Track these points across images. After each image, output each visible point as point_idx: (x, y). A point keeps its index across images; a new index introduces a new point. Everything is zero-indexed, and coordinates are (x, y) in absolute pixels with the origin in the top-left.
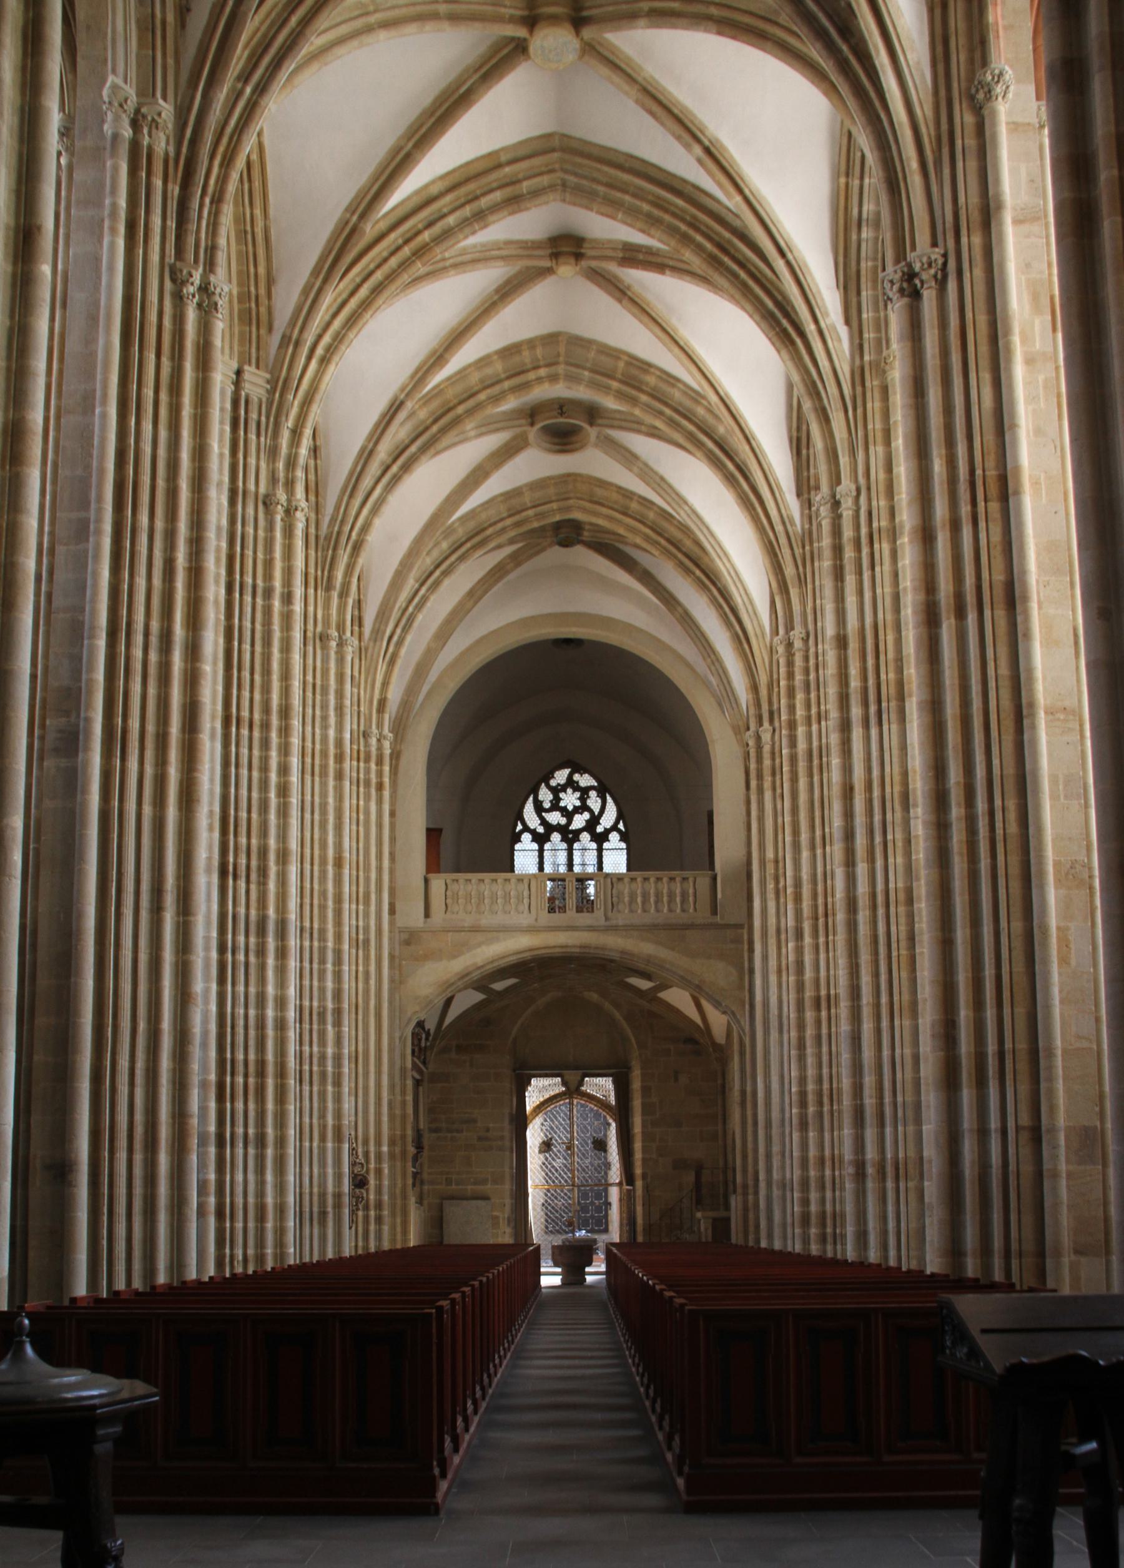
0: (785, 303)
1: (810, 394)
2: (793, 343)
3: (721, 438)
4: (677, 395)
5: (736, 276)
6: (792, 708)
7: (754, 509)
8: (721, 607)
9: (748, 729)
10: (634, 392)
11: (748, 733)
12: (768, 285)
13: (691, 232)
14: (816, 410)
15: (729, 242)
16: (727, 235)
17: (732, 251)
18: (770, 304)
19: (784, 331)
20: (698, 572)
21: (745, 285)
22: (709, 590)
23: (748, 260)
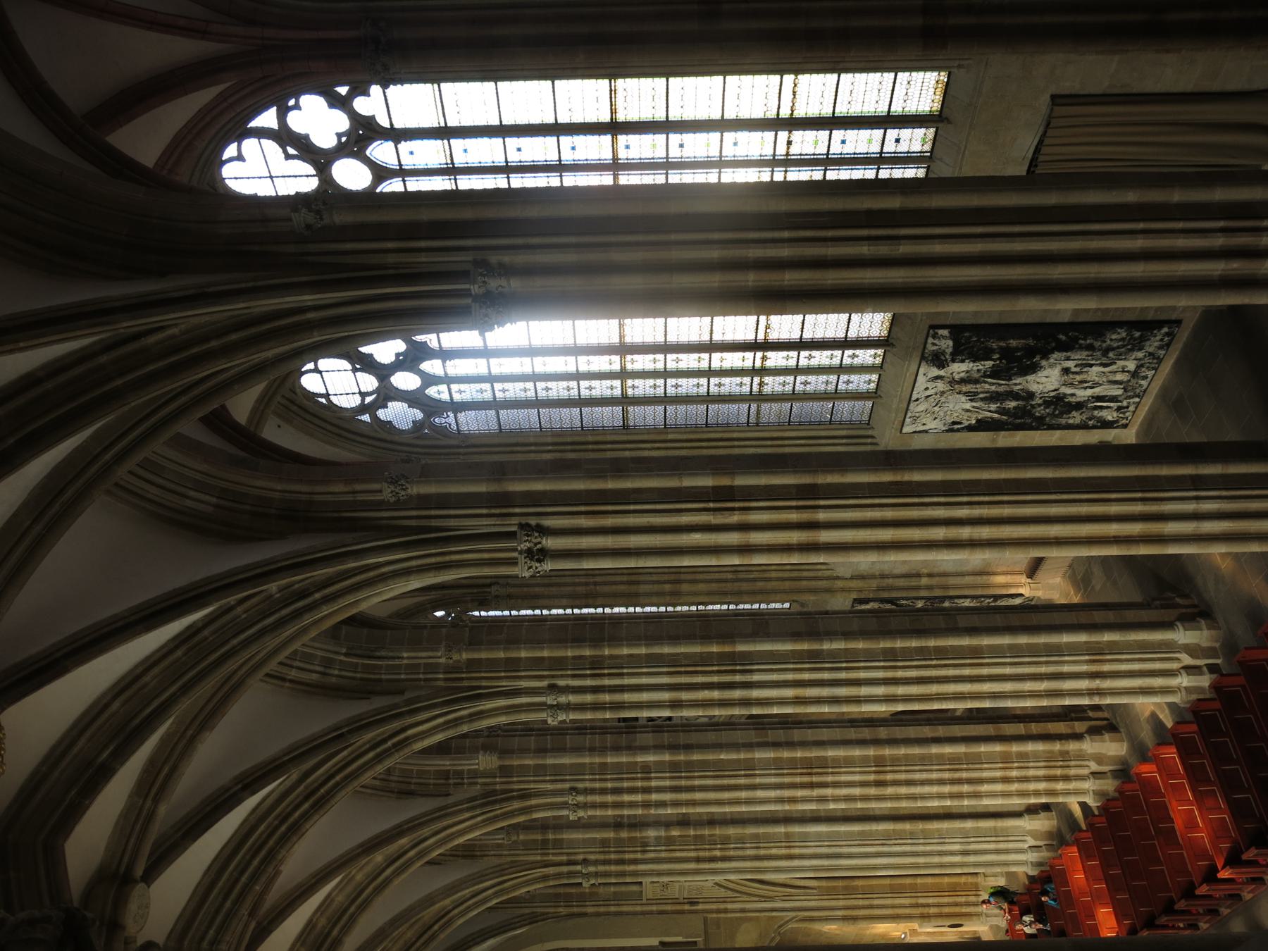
0: (372, 743)
1: (456, 725)
2: (407, 739)
3: (386, 861)
4: (340, 898)
5: (338, 784)
6: (632, 805)
7: (452, 834)
8: (469, 907)
9: (581, 884)
10: (329, 940)
11: (585, 884)
12: (352, 756)
13: (291, 820)
14: (470, 721)
15: (306, 788)
16: (302, 787)
17: (316, 785)
18: (371, 755)
19: (394, 745)
20: (436, 927)
21: (346, 778)
22: (453, 917)
23: (327, 771)
